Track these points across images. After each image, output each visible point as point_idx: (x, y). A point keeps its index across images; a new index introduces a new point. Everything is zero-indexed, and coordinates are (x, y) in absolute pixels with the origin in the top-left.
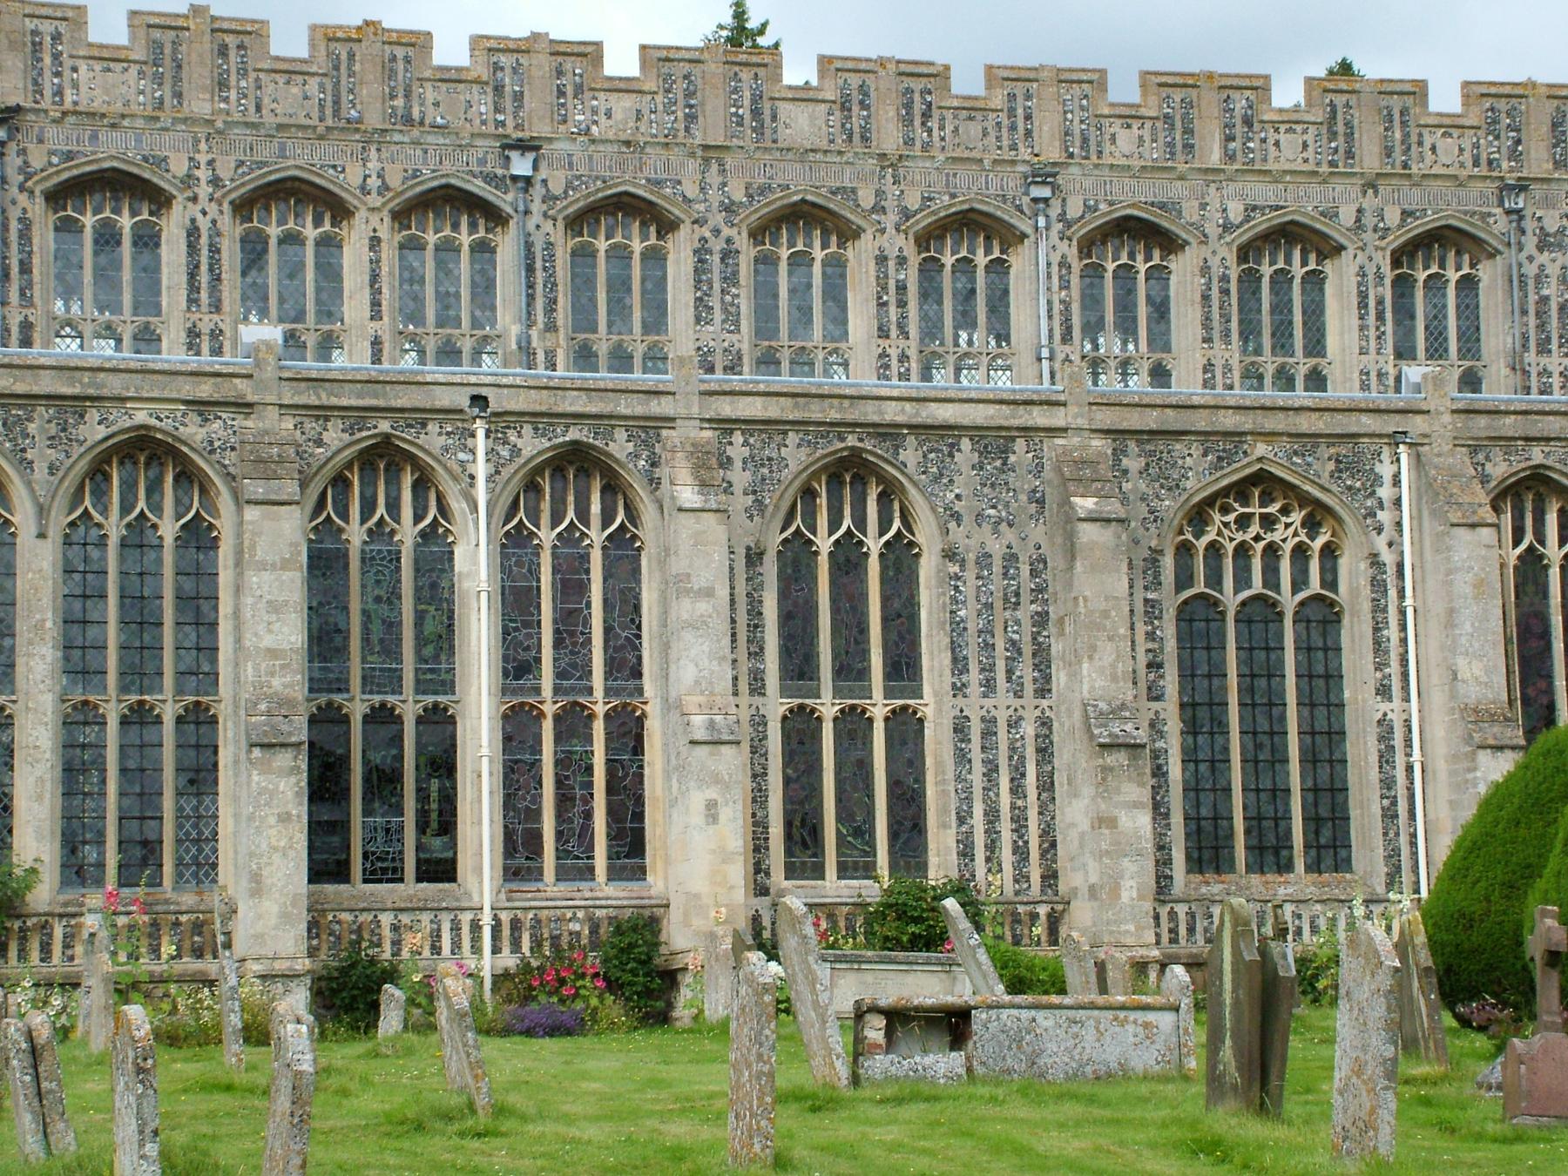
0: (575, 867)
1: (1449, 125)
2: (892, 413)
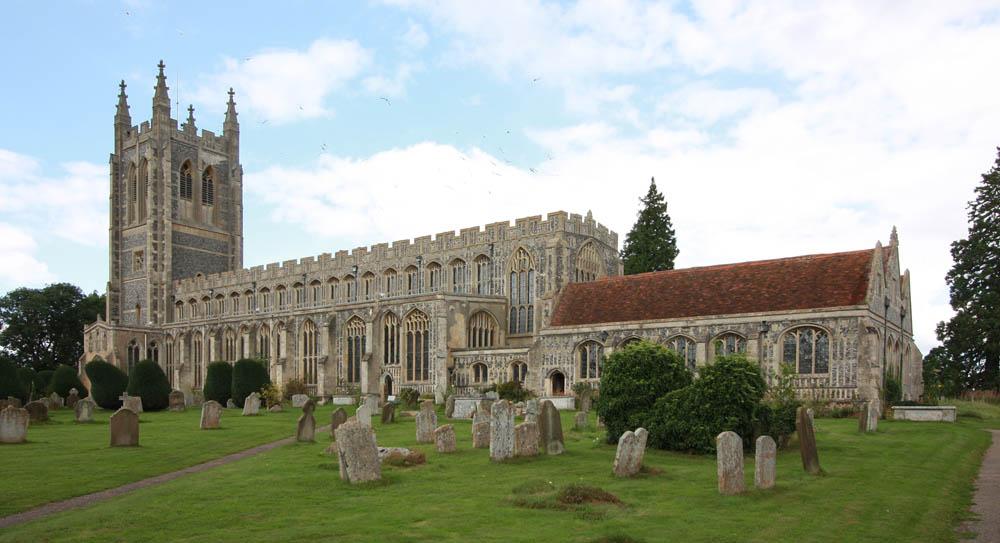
0: (311, 382)
1: (483, 234)
2: (314, 311)
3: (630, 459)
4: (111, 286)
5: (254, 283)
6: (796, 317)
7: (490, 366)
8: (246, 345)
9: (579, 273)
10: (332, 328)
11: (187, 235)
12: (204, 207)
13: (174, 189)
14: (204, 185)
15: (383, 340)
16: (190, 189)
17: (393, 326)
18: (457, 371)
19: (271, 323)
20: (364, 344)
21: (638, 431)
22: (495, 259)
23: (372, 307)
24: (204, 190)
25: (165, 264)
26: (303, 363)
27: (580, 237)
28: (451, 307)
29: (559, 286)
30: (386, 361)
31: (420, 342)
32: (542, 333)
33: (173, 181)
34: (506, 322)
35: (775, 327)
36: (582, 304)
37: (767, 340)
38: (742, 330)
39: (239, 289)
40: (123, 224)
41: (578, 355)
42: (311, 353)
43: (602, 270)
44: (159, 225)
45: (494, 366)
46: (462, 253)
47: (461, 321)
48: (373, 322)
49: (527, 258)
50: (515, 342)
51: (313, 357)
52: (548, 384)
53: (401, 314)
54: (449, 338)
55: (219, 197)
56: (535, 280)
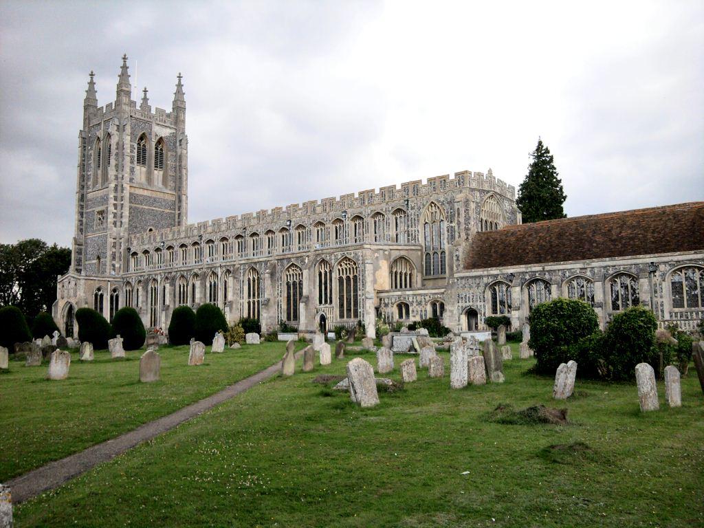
1: (399, 191)
2: (256, 260)
3: (565, 386)
4: (76, 242)
5: (201, 236)
6: (680, 258)
7: (412, 303)
8: (197, 291)
9: (484, 222)
10: (272, 275)
11: (141, 196)
12: (156, 172)
13: (132, 158)
14: (156, 153)
15: (318, 284)
16: (144, 158)
17: (326, 272)
18: (383, 310)
19: (219, 271)
20: (301, 288)
21: (571, 362)
22: (410, 212)
23: (308, 256)
24: (156, 158)
25: (124, 220)
26: (247, 304)
27: (482, 191)
28: (376, 255)
29: (467, 235)
30: (321, 302)
31: (351, 284)
32: (456, 275)
33: (132, 151)
34: (422, 265)
35: (662, 267)
36: (491, 251)
37: (657, 278)
38: (634, 270)
39: (188, 241)
40: (88, 188)
41: (489, 294)
42: (254, 295)
43: (507, 217)
44: (119, 188)
45: (415, 304)
46: (382, 207)
47: (384, 266)
48: (309, 269)
49: (438, 210)
50: (430, 284)
51: (256, 300)
52: (464, 319)
53: (333, 261)
54: (375, 281)
55: (170, 162)
56: (446, 229)
